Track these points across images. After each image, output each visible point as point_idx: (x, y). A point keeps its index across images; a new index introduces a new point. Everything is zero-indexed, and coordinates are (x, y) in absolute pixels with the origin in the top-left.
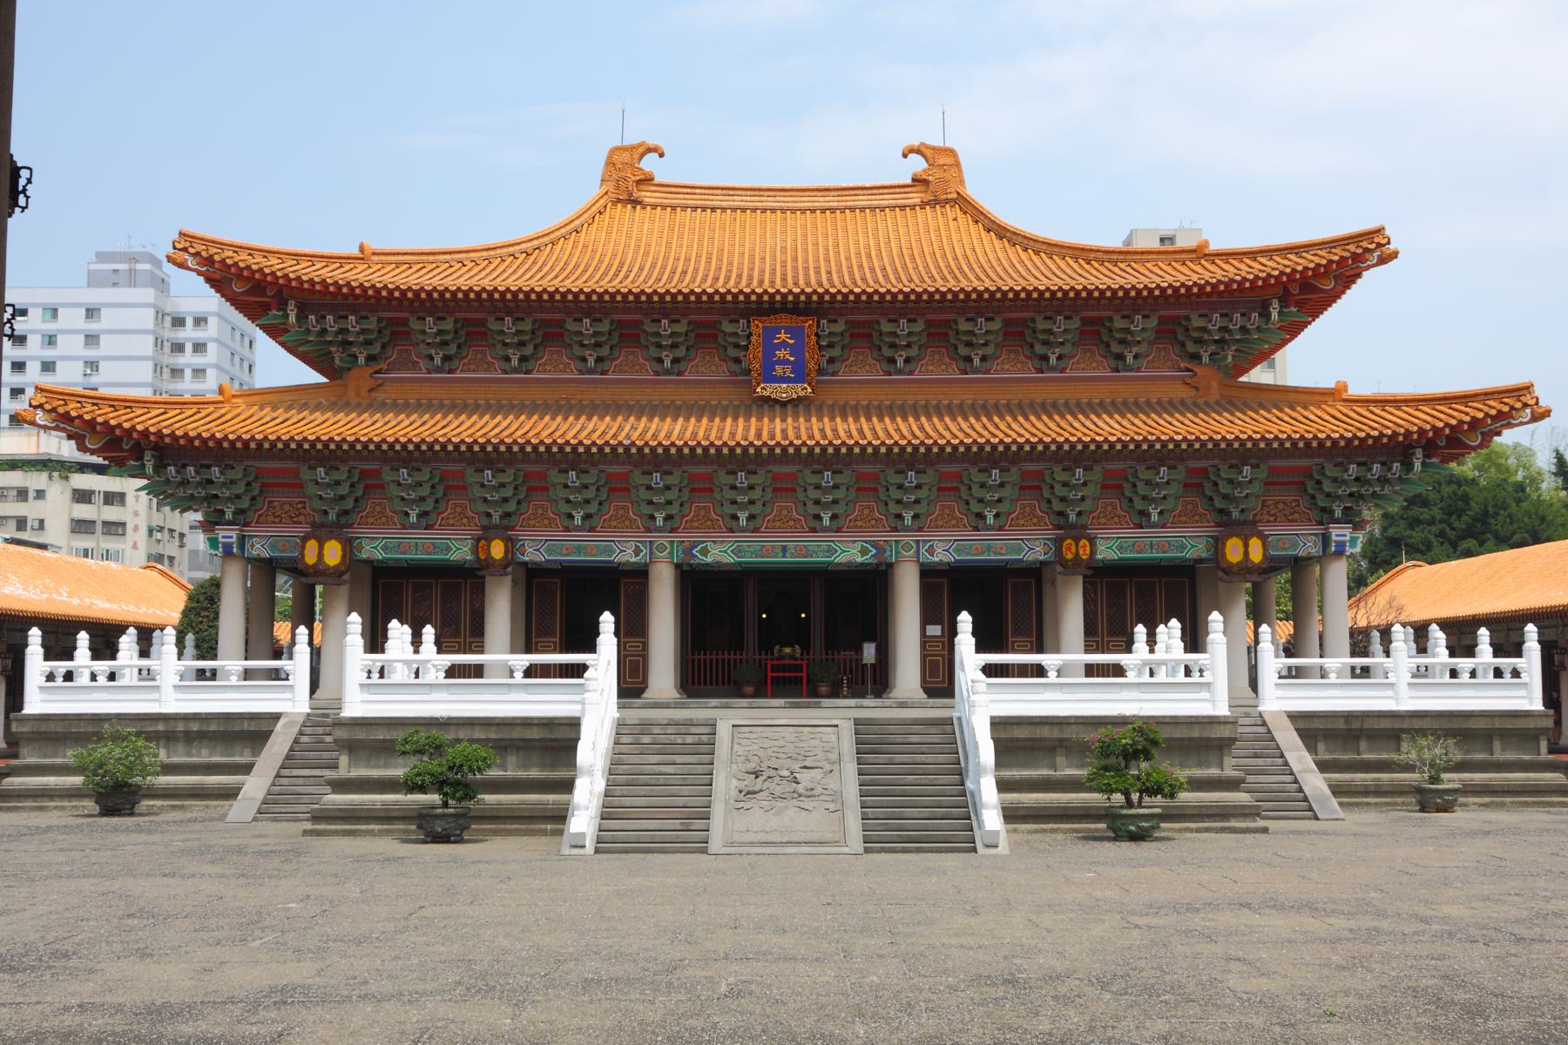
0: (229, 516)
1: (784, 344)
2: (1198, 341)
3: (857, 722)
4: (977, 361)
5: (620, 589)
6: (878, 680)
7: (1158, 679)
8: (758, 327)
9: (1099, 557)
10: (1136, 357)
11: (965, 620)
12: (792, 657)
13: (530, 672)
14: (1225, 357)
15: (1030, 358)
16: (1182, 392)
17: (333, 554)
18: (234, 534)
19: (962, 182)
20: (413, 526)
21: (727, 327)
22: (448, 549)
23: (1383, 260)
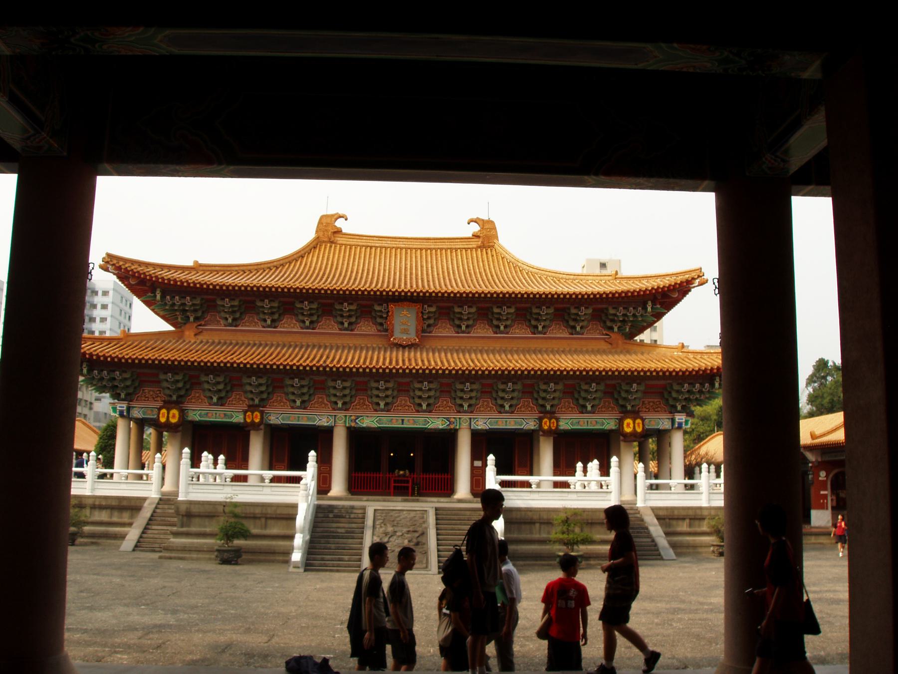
0: (123, 396)
2: (612, 321)
3: (436, 509)
4: (502, 328)
5: (321, 439)
6: (447, 488)
7: (587, 489)
9: (561, 428)
10: (581, 328)
11: (491, 458)
12: (404, 475)
13: (274, 480)
15: (529, 327)
16: (603, 345)
17: (174, 416)
18: (125, 406)
19: (497, 238)
20: (215, 404)
21: (377, 308)
22: (232, 417)
23: (701, 284)
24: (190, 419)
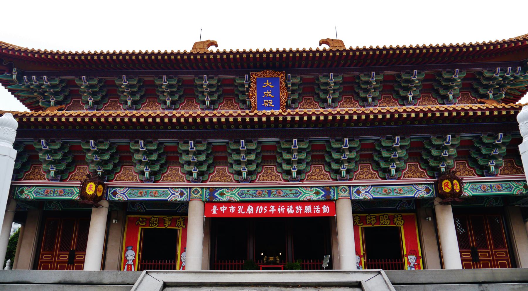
1: (268, 88)
8: (254, 77)
14: (501, 95)
24: (23, 197)
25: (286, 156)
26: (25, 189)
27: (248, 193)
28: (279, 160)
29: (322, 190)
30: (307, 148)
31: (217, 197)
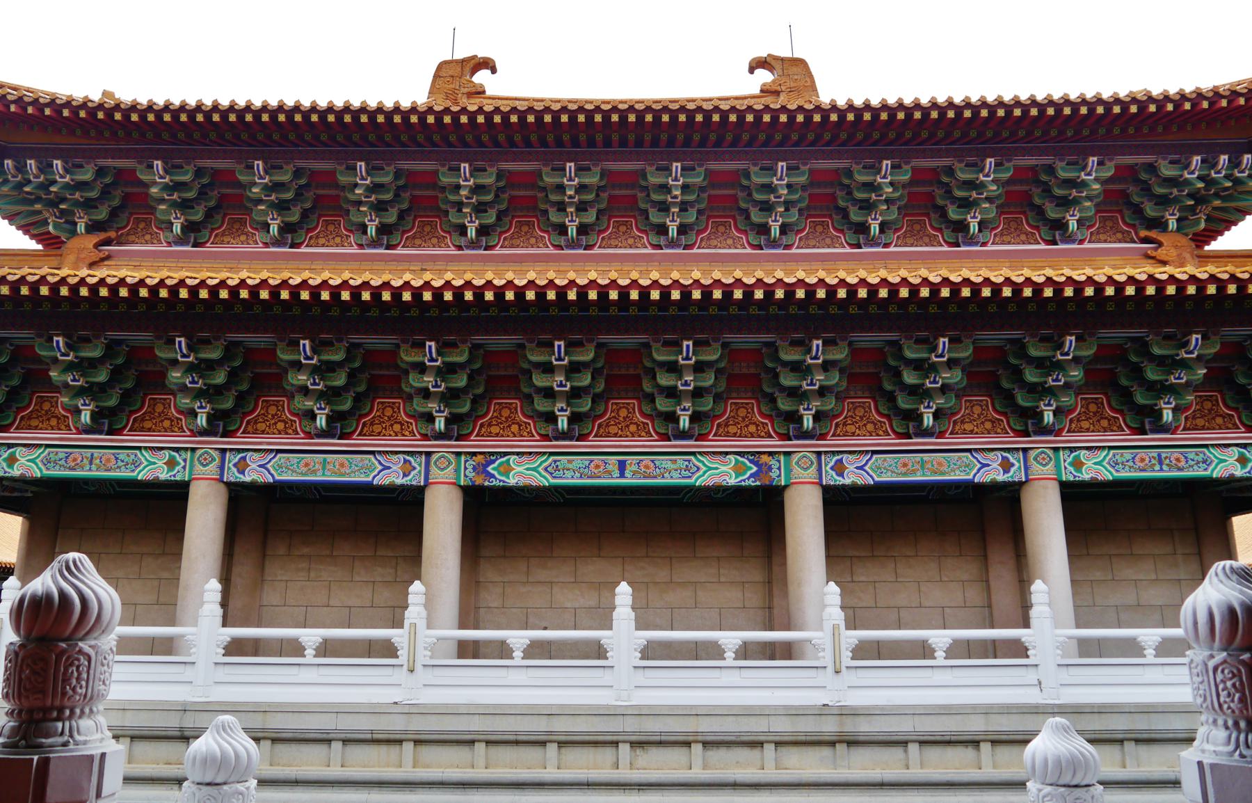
14: (1198, 221)
25: (664, 380)
26: (19, 451)
27: (570, 466)
28: (647, 387)
29: (751, 461)
30: (717, 361)
31: (493, 476)
